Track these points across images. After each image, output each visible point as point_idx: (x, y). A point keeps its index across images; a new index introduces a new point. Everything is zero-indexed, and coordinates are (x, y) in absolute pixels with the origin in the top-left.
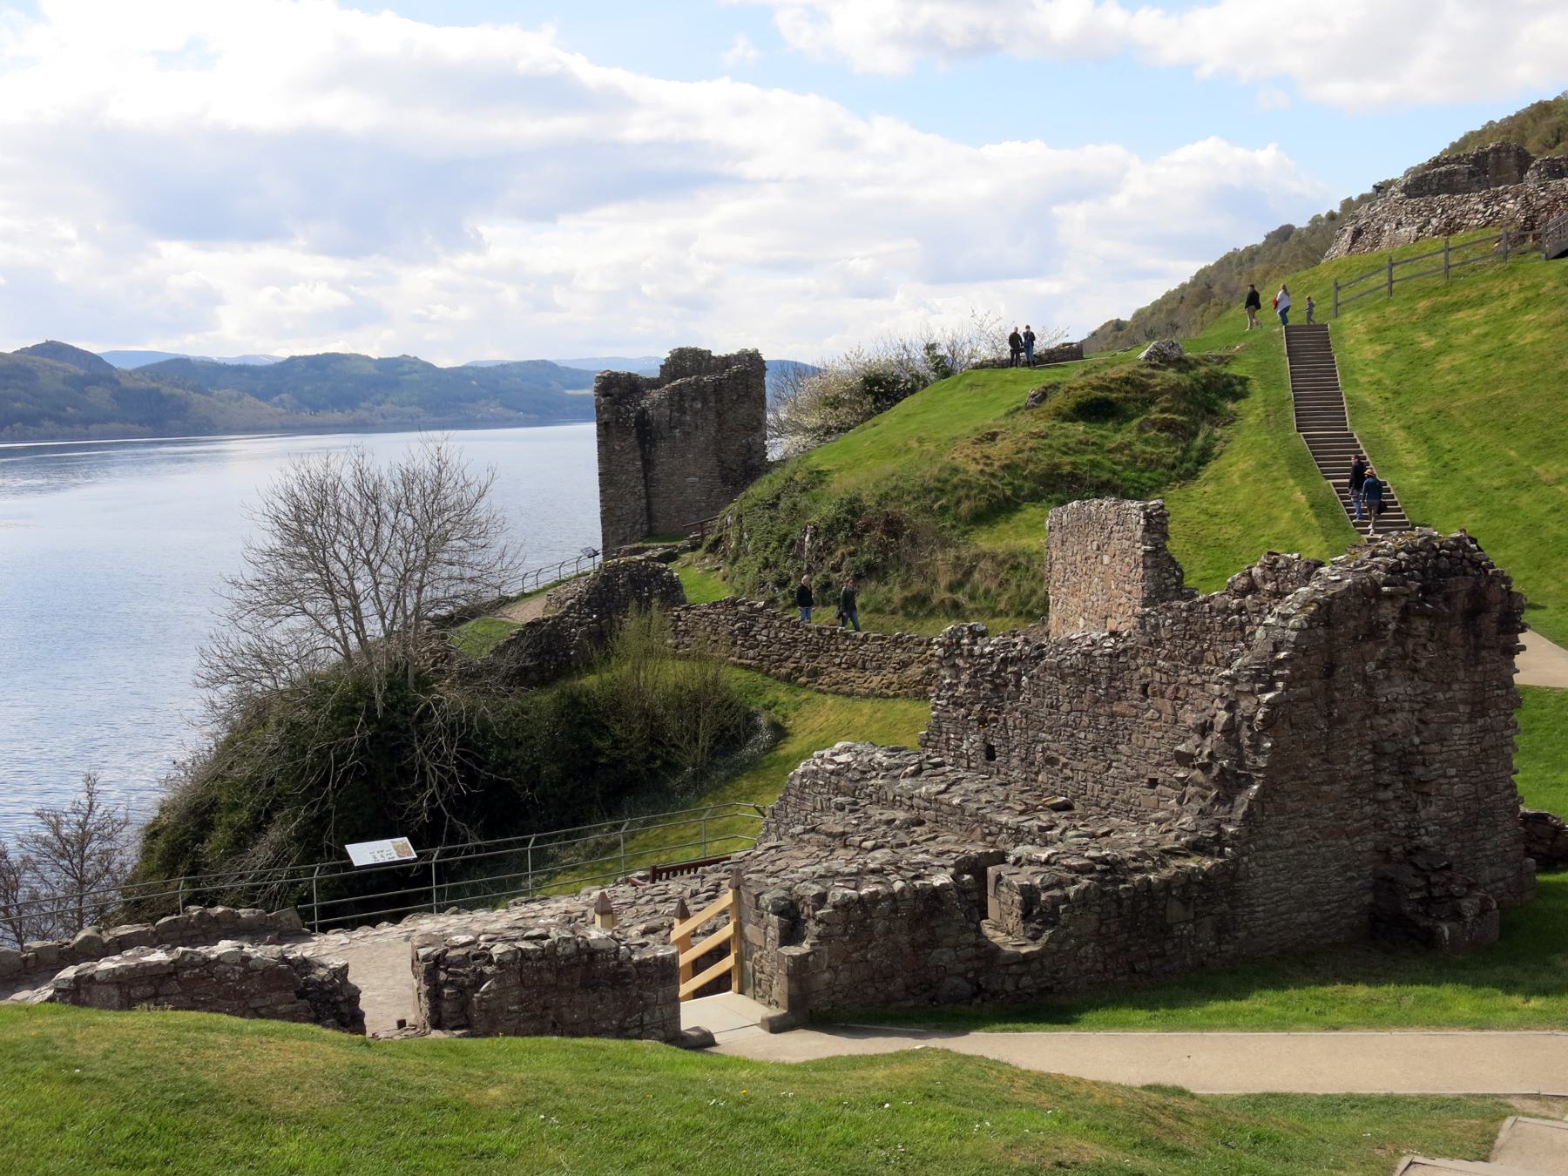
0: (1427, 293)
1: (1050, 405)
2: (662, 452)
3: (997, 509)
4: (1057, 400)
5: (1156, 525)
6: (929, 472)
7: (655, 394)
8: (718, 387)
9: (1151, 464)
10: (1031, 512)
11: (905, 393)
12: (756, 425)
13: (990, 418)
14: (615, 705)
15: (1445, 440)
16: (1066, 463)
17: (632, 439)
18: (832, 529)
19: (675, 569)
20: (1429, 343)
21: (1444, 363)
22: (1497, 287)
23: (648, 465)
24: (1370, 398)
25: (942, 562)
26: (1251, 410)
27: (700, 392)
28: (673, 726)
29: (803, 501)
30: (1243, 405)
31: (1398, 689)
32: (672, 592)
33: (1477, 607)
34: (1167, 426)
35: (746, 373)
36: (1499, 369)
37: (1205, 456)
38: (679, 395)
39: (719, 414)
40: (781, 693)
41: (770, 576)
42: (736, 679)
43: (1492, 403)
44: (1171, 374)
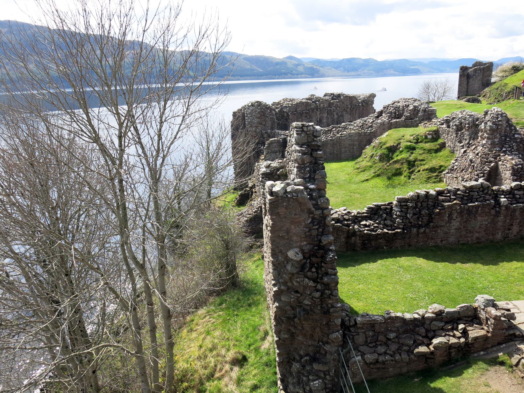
2: (471, 80)
8: (484, 68)
11: (520, 70)
12: (490, 76)
17: (466, 78)
18: (509, 93)
23: (468, 83)
27: (480, 69)
29: (504, 88)
38: (475, 70)
39: (483, 73)
41: (497, 100)
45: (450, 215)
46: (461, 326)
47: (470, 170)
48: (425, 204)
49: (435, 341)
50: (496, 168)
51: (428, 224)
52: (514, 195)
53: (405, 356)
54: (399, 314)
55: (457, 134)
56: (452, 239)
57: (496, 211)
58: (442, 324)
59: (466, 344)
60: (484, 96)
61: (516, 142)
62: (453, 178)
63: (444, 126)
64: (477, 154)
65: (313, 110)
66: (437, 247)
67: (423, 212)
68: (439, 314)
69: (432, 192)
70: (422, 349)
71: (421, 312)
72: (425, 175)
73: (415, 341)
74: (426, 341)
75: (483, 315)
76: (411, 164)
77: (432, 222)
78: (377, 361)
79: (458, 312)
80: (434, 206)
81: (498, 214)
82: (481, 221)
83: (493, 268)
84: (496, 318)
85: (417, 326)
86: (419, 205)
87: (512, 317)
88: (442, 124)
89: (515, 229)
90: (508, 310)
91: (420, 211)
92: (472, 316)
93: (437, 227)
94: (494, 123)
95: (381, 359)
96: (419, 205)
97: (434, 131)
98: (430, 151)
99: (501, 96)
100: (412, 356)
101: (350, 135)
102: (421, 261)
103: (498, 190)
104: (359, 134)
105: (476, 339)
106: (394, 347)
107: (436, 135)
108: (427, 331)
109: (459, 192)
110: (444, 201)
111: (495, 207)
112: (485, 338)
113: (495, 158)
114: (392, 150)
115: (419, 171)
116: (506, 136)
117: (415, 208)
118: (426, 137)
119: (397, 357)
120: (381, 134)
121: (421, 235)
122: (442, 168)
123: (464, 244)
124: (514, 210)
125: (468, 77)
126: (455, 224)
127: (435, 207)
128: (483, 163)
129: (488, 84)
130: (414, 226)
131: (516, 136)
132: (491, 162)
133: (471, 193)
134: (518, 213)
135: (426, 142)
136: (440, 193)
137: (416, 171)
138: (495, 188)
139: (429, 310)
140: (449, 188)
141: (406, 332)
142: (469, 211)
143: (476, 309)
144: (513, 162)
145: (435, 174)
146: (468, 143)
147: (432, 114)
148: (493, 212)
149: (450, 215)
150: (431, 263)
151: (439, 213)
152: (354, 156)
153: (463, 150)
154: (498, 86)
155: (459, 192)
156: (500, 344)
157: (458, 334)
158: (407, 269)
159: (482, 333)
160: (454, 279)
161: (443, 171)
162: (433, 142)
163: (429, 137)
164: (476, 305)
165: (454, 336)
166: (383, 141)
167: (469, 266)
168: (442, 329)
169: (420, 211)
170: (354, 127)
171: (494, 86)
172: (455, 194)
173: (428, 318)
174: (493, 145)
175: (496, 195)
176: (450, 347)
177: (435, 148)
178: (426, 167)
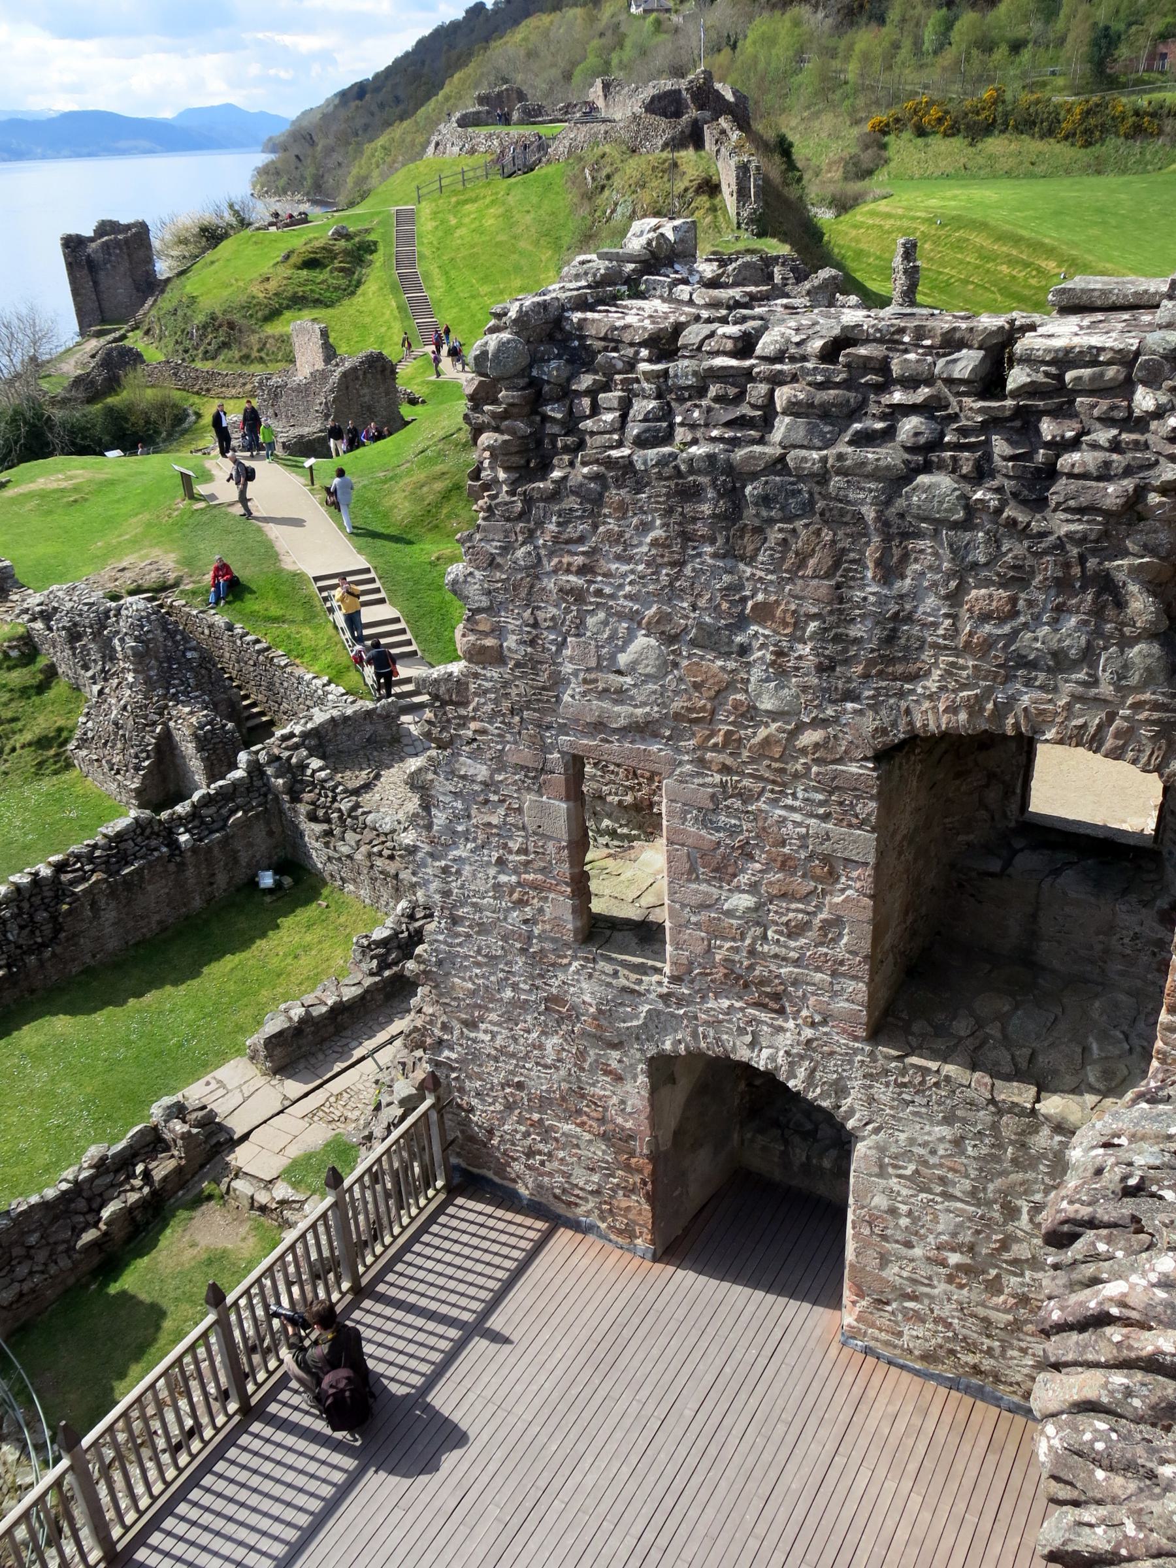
0: (455, 193)
1: (294, 259)
3: (273, 314)
4: (294, 259)
5: (324, 334)
6: (243, 298)
7: (93, 245)
8: (126, 240)
9: (337, 289)
10: (288, 314)
12: (149, 261)
13: (266, 268)
14: (131, 407)
15: (453, 274)
16: (300, 291)
18: (205, 327)
19: (127, 343)
20: (453, 222)
21: (458, 233)
22: (483, 192)
23: (96, 283)
24: (427, 251)
25: (254, 339)
26: (378, 258)
27: (117, 243)
28: (154, 416)
30: (374, 257)
31: (366, 391)
32: (137, 358)
33: (383, 371)
34: (342, 270)
35: (141, 231)
36: (477, 238)
37: (359, 283)
40: (196, 399)
41: (180, 348)
42: (177, 395)
43: (472, 255)
44: (342, 243)
45: (93, 904)
46: (139, 1168)
47: (119, 745)
48: (37, 900)
49: (105, 1214)
50: (167, 735)
51: (55, 937)
52: (202, 817)
53: (65, 1263)
54: (34, 1199)
55: (73, 649)
56: (112, 944)
57: (178, 864)
58: (108, 1179)
59: (153, 1193)
60: (147, 333)
61: (192, 669)
62: (91, 761)
63: (39, 625)
64: (124, 708)
66: (88, 971)
67: (38, 918)
68: (101, 1165)
69: (45, 871)
70: (89, 1236)
71: (69, 1174)
72: (28, 758)
73: (73, 1229)
74: (91, 1218)
75: (168, 1136)
77: (61, 930)
78: (21, 1295)
79: (130, 1147)
80: (56, 897)
81: (182, 866)
82: (156, 891)
83: (195, 983)
84: (186, 1136)
85: (72, 1201)
86: (26, 905)
87: (212, 1115)
88: (33, 620)
89: (222, 879)
90: (204, 1107)
91: (31, 916)
92: (152, 1143)
93: (74, 935)
94: (137, 639)
95: (26, 1287)
96: (26, 905)
97: (21, 638)
98: (24, 692)
99: (189, 336)
100: (76, 1256)
102: (61, 1024)
103: (171, 819)
105: (165, 1179)
106: (41, 1256)
108: (89, 1200)
109: (98, 853)
110: (73, 883)
111: (172, 855)
112: (179, 1170)
113: (161, 714)
115: (13, 750)
116: (169, 660)
117: (20, 914)
118: (7, 656)
119: (53, 1270)
121: (48, 965)
122: (65, 734)
123: (137, 944)
124: (209, 849)
125: (92, 266)
126: (110, 915)
127: (58, 899)
128: (140, 729)
129: (150, 286)
130: (30, 951)
131: (189, 655)
132: (154, 724)
133: (122, 846)
134: (216, 851)
135: (9, 669)
136: (60, 868)
137: (7, 749)
138: (164, 815)
139: (79, 1168)
140: (75, 848)
141: (56, 1218)
142: (127, 883)
143: (155, 1128)
144: (194, 720)
145: (52, 752)
146: (103, 670)
147: (5, 579)
148: (172, 867)
149: (93, 904)
150: (82, 1019)
151: (70, 911)
153: (96, 688)
154: (175, 303)
155: (98, 853)
156: (202, 1166)
157: (137, 1182)
158: (36, 1056)
159: (171, 1164)
160: (128, 1044)
161: (66, 741)
162: (25, 665)
163: (14, 653)
164: (154, 1120)
165: (133, 1189)
167: (149, 998)
168: (112, 1185)
169: (31, 916)
171: (167, 301)
172: (91, 859)
173: (86, 1179)
174: (148, 681)
175: (168, 832)
176: (129, 1211)
177: (35, 682)
178: (28, 736)
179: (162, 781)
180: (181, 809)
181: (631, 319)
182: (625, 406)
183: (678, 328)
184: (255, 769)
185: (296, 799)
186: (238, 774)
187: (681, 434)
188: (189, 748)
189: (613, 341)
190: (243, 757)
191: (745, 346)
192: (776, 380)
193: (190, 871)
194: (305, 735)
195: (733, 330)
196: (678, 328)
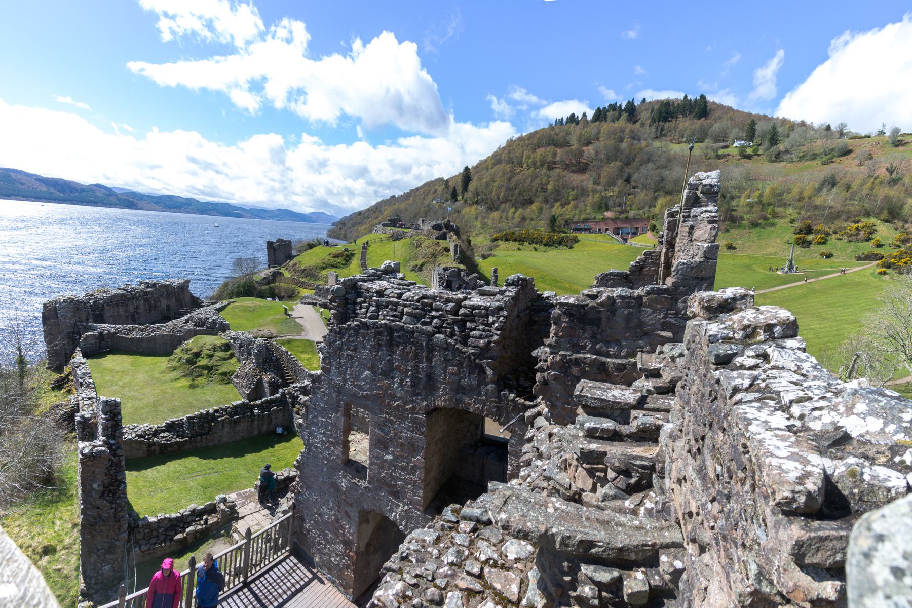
65: (129, 299)
71: (182, 511)
76: (210, 369)
81: (253, 421)
101: (163, 336)
104: (171, 336)
107: (227, 347)
114: (197, 355)
120: (188, 339)
124: (263, 417)
139: (185, 510)
152: (168, 353)
166: (189, 346)
170: (166, 328)
179: (257, 392)
180: (258, 402)
181: (374, 286)
182: (368, 308)
183: (386, 289)
184: (283, 395)
185: (294, 407)
186: (278, 395)
187: (381, 317)
188: (266, 385)
189: (368, 290)
190: (281, 390)
191: (399, 296)
192: (405, 306)
193: (256, 422)
194: (300, 387)
195: (398, 291)
196: (386, 289)
